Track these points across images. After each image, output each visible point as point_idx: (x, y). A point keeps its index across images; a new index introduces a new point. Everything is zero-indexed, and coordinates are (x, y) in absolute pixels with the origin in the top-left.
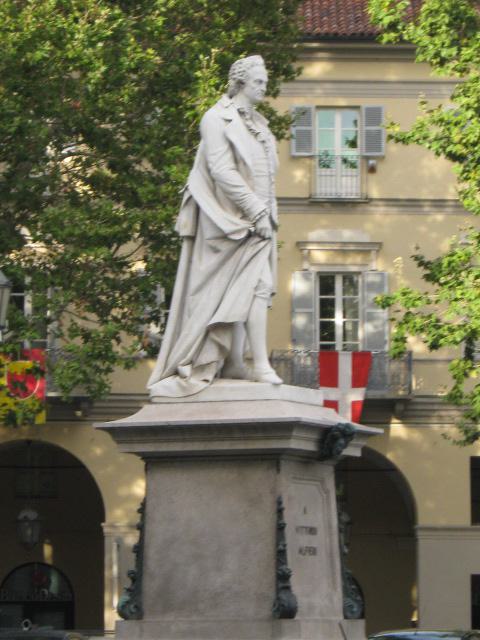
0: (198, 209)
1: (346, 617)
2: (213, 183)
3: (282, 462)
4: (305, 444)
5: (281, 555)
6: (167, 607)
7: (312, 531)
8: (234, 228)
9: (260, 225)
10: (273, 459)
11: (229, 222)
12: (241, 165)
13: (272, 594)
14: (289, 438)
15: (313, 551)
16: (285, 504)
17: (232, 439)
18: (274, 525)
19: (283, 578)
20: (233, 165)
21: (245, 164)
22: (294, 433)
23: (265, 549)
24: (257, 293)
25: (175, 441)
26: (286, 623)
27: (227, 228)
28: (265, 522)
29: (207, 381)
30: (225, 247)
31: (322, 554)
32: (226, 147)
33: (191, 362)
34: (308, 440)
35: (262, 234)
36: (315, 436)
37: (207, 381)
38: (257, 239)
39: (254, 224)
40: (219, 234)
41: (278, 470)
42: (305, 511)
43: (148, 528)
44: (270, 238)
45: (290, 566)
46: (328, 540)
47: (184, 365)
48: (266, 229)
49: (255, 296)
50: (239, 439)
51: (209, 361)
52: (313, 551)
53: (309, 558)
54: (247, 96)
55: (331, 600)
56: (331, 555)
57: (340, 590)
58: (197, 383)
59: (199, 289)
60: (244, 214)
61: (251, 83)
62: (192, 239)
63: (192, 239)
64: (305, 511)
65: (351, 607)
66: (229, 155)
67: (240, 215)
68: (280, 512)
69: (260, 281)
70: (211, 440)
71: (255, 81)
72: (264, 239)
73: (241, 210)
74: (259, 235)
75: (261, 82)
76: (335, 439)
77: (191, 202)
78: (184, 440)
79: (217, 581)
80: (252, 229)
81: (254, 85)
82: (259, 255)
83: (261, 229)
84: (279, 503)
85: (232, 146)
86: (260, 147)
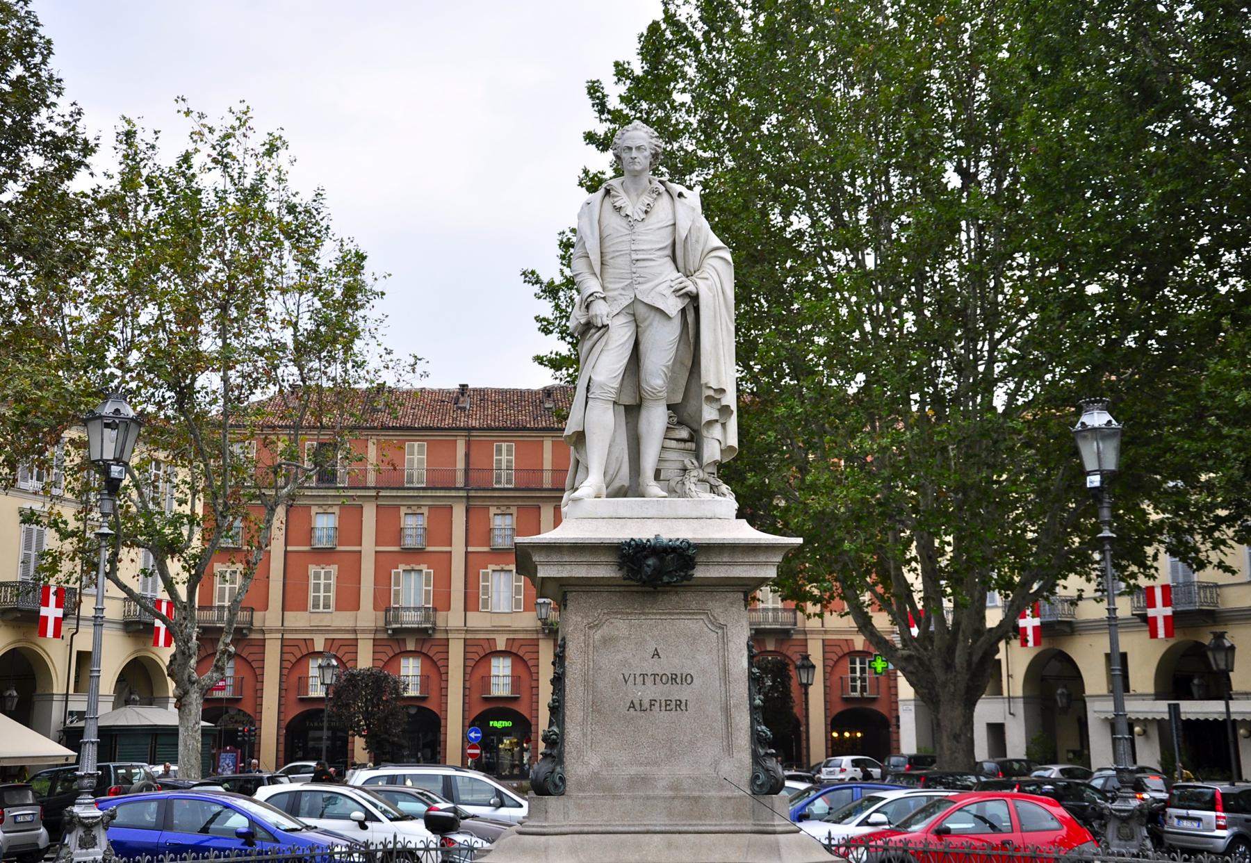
3: (569, 596)
4: (604, 571)
15: (679, 704)
42: (656, 654)
44: (604, 326)
46: (723, 689)
57: (746, 758)
64: (656, 654)
75: (630, 149)
86: (624, 223)
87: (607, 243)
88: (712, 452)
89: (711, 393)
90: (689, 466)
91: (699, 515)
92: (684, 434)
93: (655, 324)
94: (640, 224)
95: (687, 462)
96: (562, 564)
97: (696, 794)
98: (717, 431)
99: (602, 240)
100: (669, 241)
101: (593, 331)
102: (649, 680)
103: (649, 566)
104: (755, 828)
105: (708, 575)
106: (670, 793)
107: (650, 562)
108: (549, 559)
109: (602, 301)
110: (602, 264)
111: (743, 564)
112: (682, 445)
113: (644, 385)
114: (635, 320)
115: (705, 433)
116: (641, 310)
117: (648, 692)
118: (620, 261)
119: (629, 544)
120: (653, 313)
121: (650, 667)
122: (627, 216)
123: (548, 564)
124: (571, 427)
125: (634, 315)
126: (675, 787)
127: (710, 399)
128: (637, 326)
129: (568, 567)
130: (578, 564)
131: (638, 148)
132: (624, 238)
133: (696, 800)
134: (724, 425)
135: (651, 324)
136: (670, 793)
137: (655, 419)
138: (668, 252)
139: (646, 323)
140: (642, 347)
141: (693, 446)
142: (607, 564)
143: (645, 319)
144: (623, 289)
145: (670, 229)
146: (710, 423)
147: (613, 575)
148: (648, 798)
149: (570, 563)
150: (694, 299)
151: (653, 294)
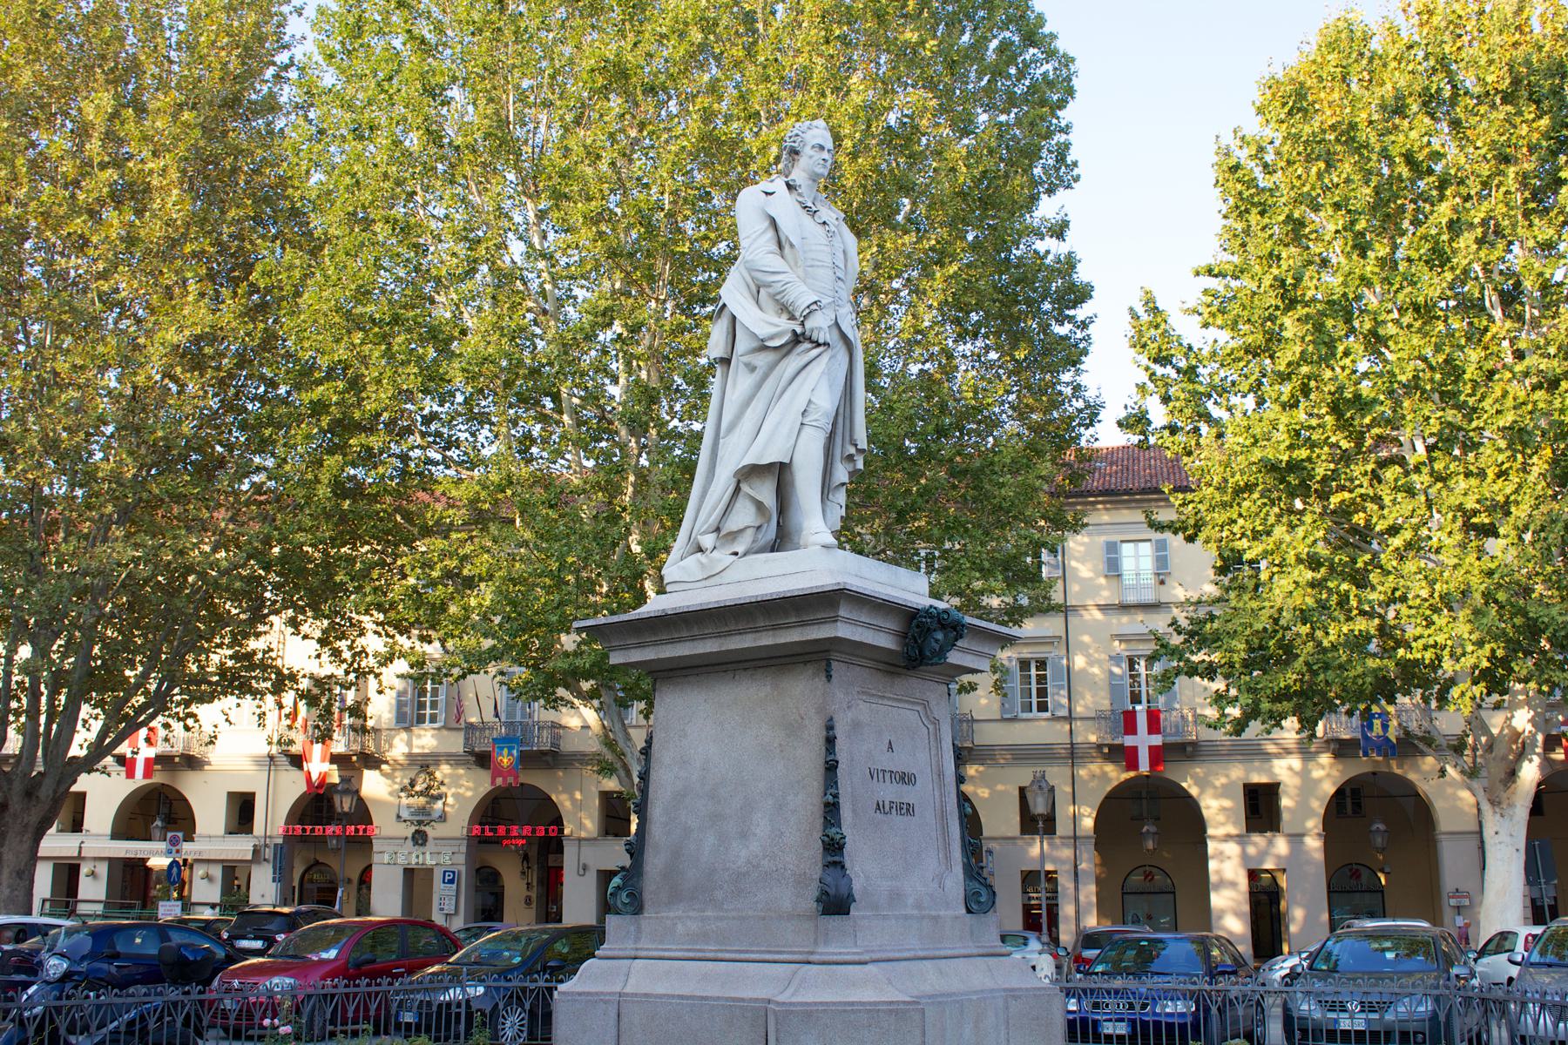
0: (734, 318)
1: (969, 911)
2: (757, 290)
3: (834, 664)
5: (831, 810)
6: (675, 896)
7: (906, 779)
8: (773, 330)
9: (808, 325)
10: (819, 657)
11: (761, 322)
12: (787, 249)
13: (816, 871)
14: (835, 620)
15: (908, 809)
16: (840, 731)
17: (756, 630)
18: (821, 762)
19: (833, 848)
20: (775, 247)
21: (792, 245)
22: (842, 613)
23: (808, 801)
25: (680, 640)
26: (835, 922)
27: (763, 331)
28: (810, 757)
29: (736, 554)
30: (762, 360)
31: (927, 816)
32: (767, 223)
33: (718, 530)
34: (879, 629)
35: (814, 337)
36: (892, 624)
37: (736, 554)
38: (807, 345)
39: (802, 324)
40: (755, 344)
41: (829, 677)
43: (653, 776)
44: (826, 344)
45: (846, 830)
47: (705, 533)
48: (820, 329)
50: (766, 629)
52: (908, 809)
53: (897, 819)
55: (941, 886)
56: (943, 816)
57: (958, 870)
58: (722, 557)
59: (732, 426)
60: (785, 309)
61: (807, 151)
62: (726, 361)
63: (726, 361)
65: (978, 894)
66: (770, 234)
67: (785, 316)
68: (830, 741)
70: (729, 634)
72: (819, 345)
73: (785, 309)
74: (810, 340)
75: (822, 148)
76: (926, 631)
77: (725, 312)
78: (693, 639)
79: (741, 854)
80: (799, 330)
81: (812, 153)
84: (830, 727)
85: (774, 223)
86: (820, 230)
89: (852, 450)
97: (933, 913)
102: (887, 776)
103: (937, 641)
104: (981, 951)
106: (915, 912)
117: (890, 792)
121: (886, 762)
123: (848, 621)
126: (919, 906)
127: (850, 458)
130: (868, 626)
133: (936, 919)
136: (915, 912)
142: (888, 632)
148: (906, 917)
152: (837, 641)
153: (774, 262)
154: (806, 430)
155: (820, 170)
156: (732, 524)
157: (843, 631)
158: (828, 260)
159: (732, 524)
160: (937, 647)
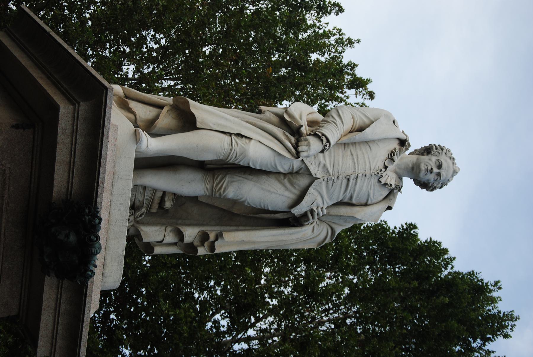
9: (311, 139)
14: (71, 101)
22: (83, 106)
24: (233, 136)
33: (126, 97)
48: (309, 145)
49: (230, 134)
51: (134, 109)
54: (417, 159)
69: (250, 139)
71: (438, 160)
72: (296, 147)
75: (440, 166)
82: (276, 141)
83: (306, 140)
86: (380, 165)
87: (365, 148)
88: (151, 233)
90: (138, 213)
91: (108, 262)
92: (168, 204)
93: (287, 194)
94: (376, 180)
95: (144, 210)
96: (74, 133)
98: (170, 238)
99: (367, 142)
100: (354, 201)
101: (293, 140)
103: (67, 236)
105: (46, 289)
107: (72, 238)
108: (81, 121)
109: (321, 148)
110: (345, 144)
111: (55, 323)
112: (157, 201)
113: (227, 179)
114: (291, 173)
115: (169, 229)
116: (303, 182)
118: (349, 162)
119: (95, 215)
120: (297, 192)
122: (386, 167)
123: (75, 117)
124: (201, 111)
125: (297, 173)
127: (204, 237)
128: (285, 175)
129: (68, 140)
130: (72, 152)
131: (439, 175)
132: (368, 165)
134: (175, 244)
135: (287, 189)
137: (191, 185)
138: (346, 200)
139: (288, 185)
140: (264, 177)
141: (155, 208)
143: (292, 184)
144: (325, 165)
145: (364, 201)
146: (180, 235)
147: (55, 189)
149: (73, 143)
150: (298, 221)
151: (316, 194)
152: (56, 108)
153: (348, 125)
154: (227, 138)
155: (423, 167)
156: (133, 105)
157: (65, 110)
158: (361, 170)
159: (133, 105)
160: (62, 237)
